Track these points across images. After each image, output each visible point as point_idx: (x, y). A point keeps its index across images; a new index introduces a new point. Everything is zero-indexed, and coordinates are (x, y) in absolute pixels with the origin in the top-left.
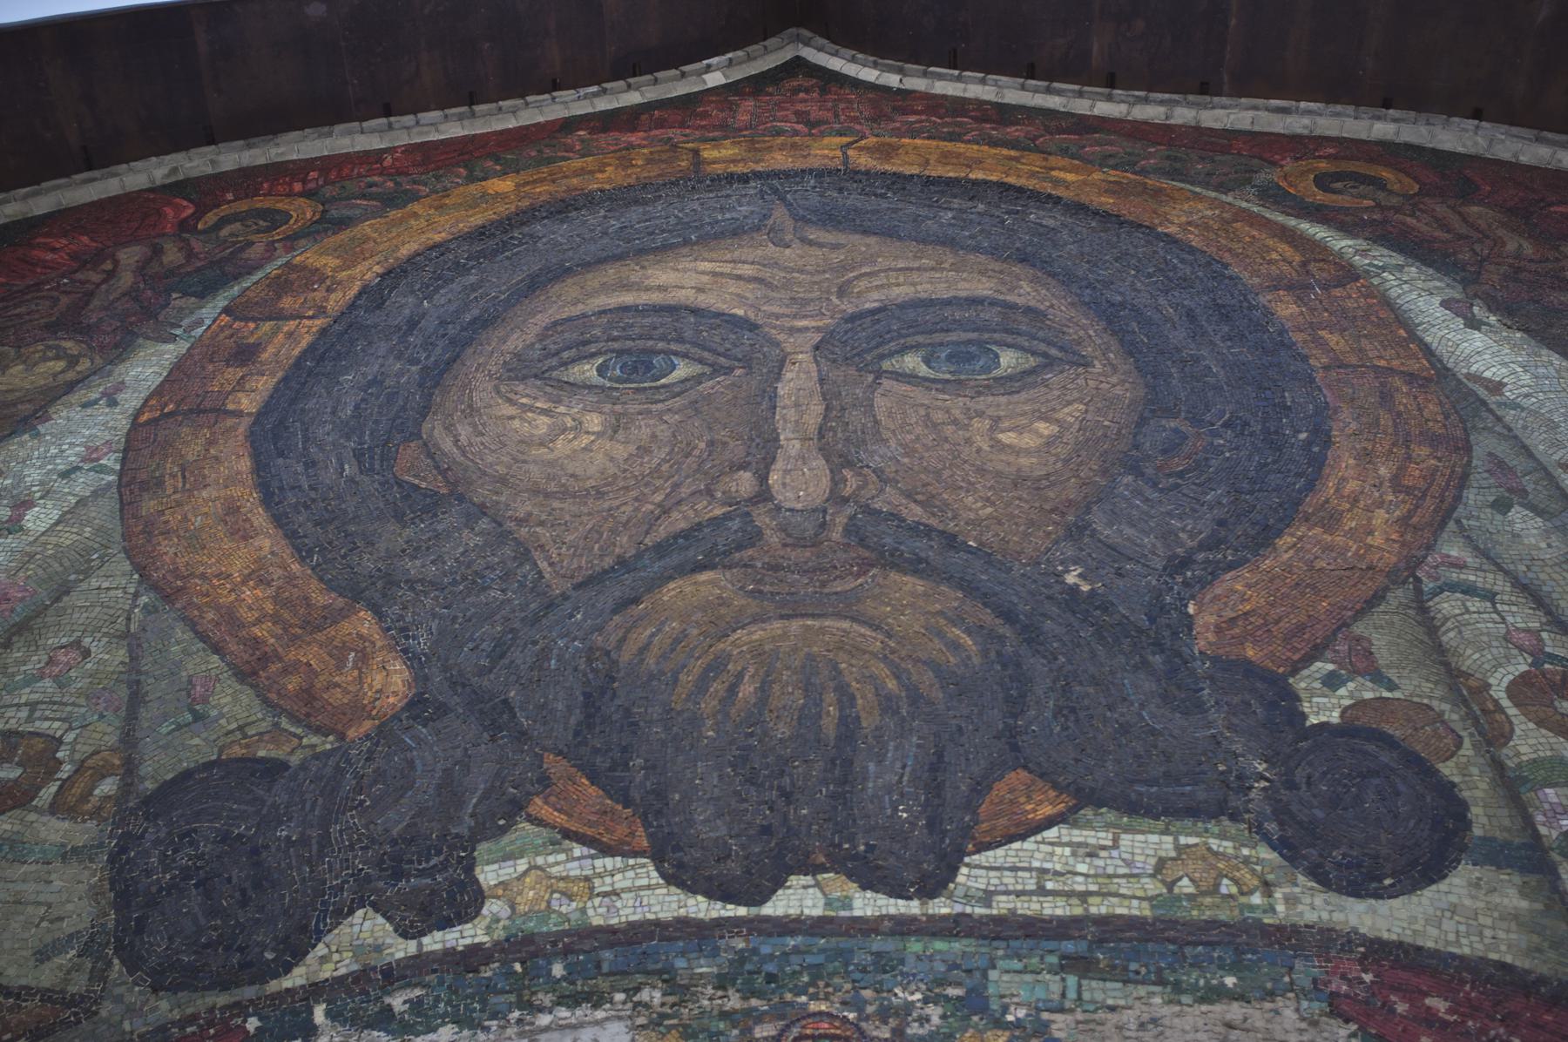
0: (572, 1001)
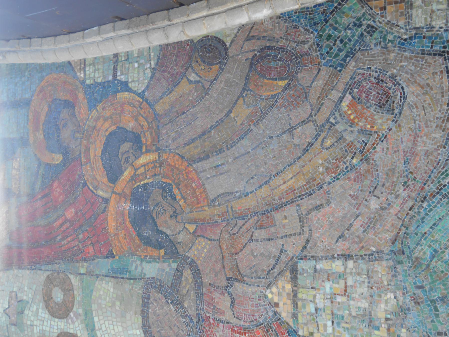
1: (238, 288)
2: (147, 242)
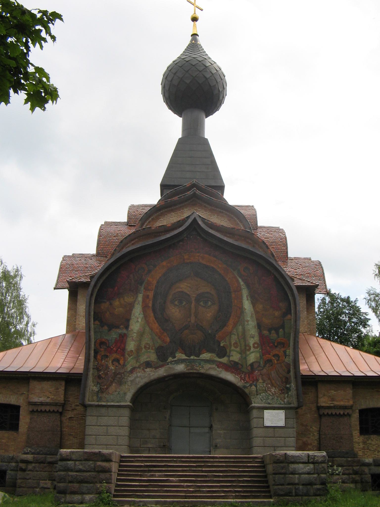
0: (181, 363)
1: (261, 375)
2: (265, 362)
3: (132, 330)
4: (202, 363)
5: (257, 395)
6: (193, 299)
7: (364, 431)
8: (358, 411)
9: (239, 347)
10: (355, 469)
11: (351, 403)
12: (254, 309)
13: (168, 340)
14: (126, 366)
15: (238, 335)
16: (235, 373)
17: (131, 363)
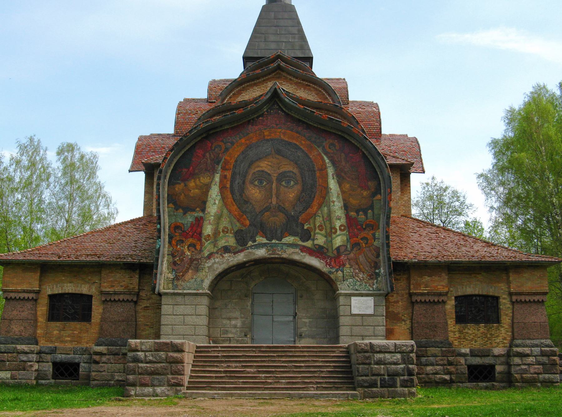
3: (209, 213)
4: (284, 247)
5: (344, 281)
6: (274, 179)
7: (460, 319)
8: (453, 298)
9: (324, 230)
10: (450, 359)
11: (446, 290)
12: (340, 189)
13: (248, 222)
14: (203, 251)
15: (323, 217)
16: (320, 258)
17: (208, 248)
